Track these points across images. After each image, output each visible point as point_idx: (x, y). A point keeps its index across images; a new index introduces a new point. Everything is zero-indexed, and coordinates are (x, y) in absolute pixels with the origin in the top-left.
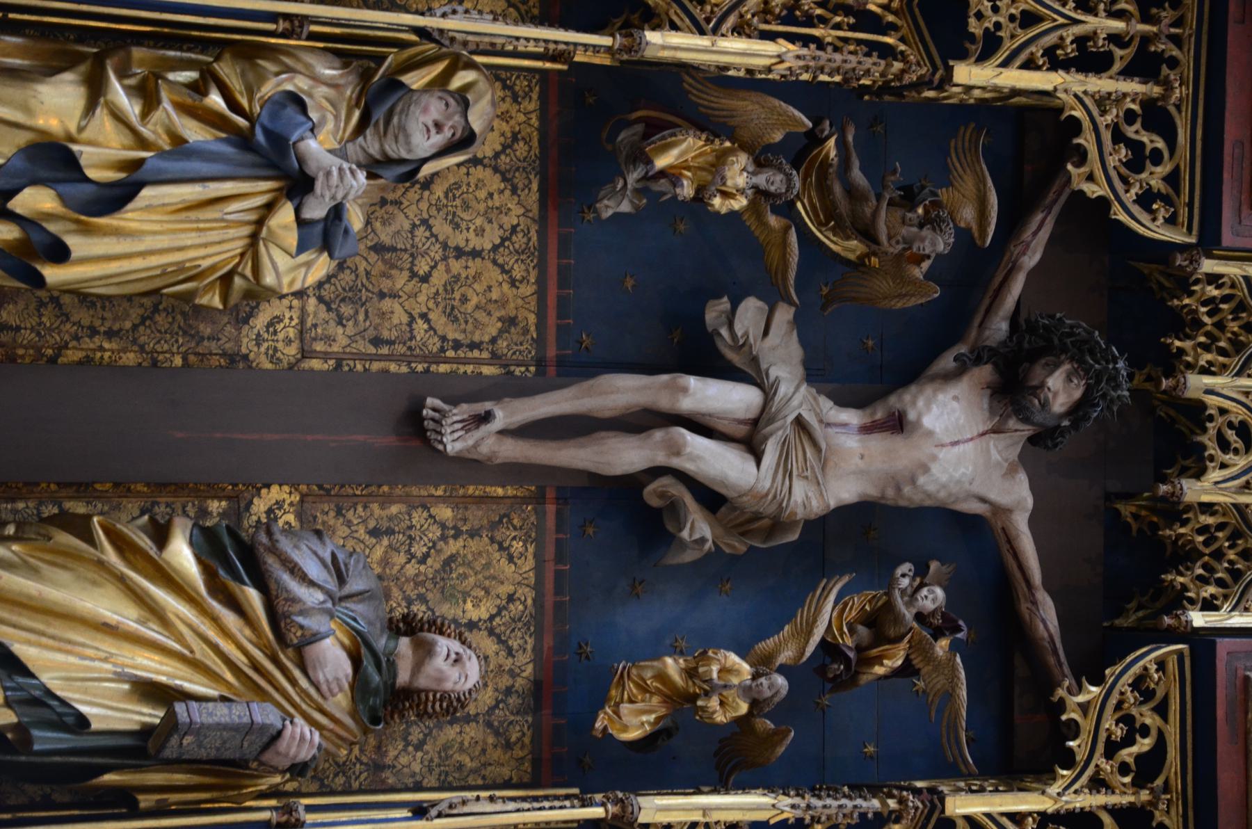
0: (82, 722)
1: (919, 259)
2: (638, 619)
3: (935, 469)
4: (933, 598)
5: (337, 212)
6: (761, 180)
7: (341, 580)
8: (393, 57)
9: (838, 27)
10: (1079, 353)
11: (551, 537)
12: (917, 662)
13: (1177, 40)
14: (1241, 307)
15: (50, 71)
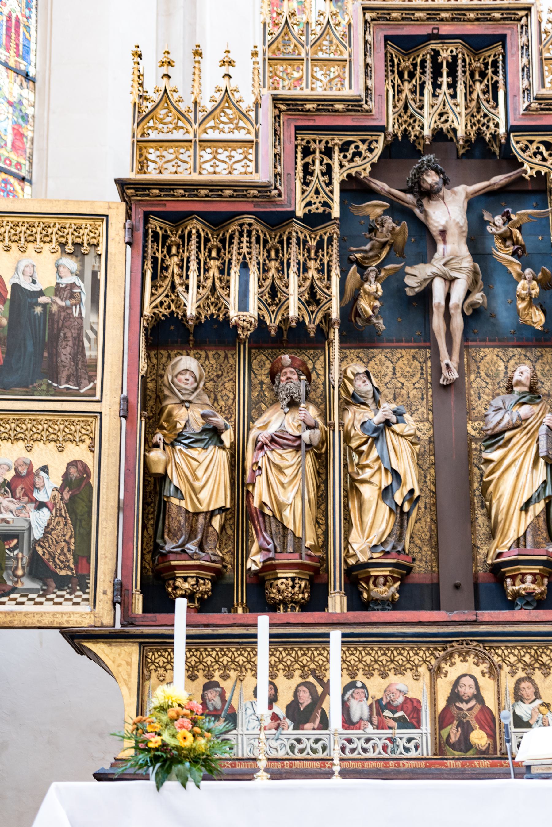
0: (545, 482)
1: (393, 228)
3: (458, 220)
4: (499, 220)
5: (394, 412)
6: (373, 280)
7: (501, 409)
8: (343, 395)
9: (323, 255)
10: (420, 172)
12: (518, 226)
13: (320, 141)
14: (400, 116)
15: (359, 494)
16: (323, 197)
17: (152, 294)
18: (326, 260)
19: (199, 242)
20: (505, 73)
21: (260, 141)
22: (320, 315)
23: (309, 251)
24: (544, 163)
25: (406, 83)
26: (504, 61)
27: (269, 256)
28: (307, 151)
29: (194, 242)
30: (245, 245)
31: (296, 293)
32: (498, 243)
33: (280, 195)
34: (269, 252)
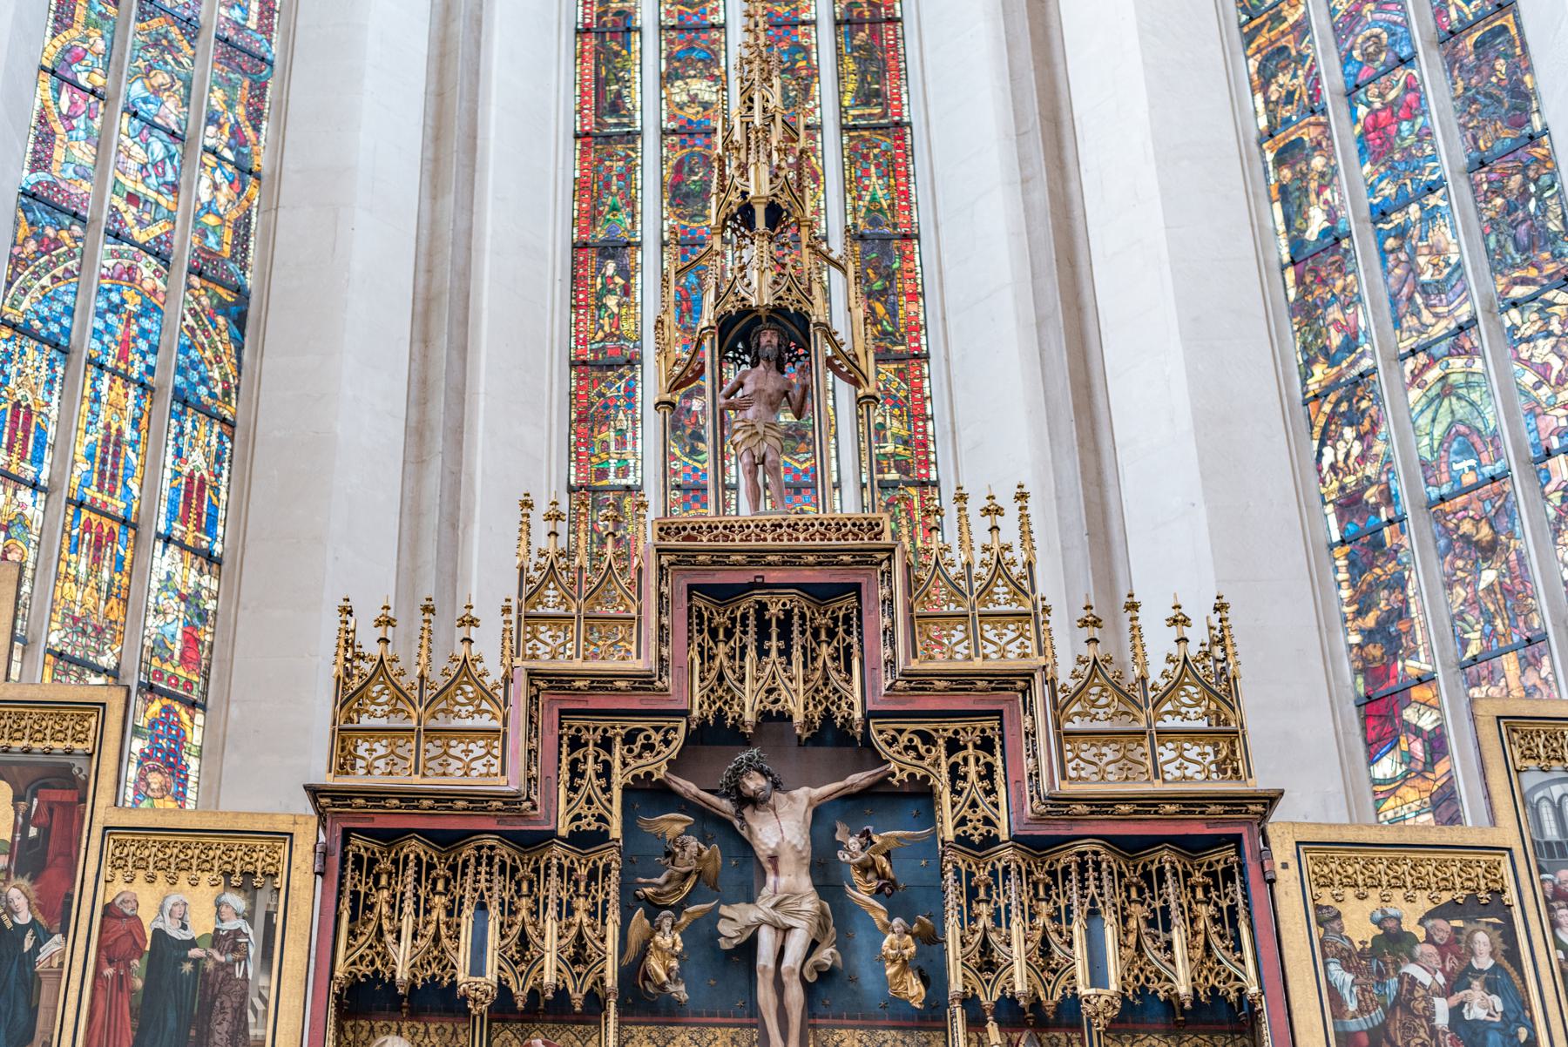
1: (700, 852)
2: (868, 980)
4: (854, 843)
6: (667, 929)
10: (737, 773)
11: (831, 1021)
13: (595, 729)
14: (712, 690)
16: (597, 808)
17: (349, 946)
18: (600, 897)
19: (418, 873)
20: (860, 633)
21: (509, 730)
22: (590, 980)
23: (577, 884)
24: (919, 763)
25: (721, 645)
26: (860, 618)
27: (518, 891)
28: (576, 743)
29: (410, 872)
30: (483, 877)
31: (555, 947)
32: (856, 877)
33: (534, 808)
34: (518, 884)
